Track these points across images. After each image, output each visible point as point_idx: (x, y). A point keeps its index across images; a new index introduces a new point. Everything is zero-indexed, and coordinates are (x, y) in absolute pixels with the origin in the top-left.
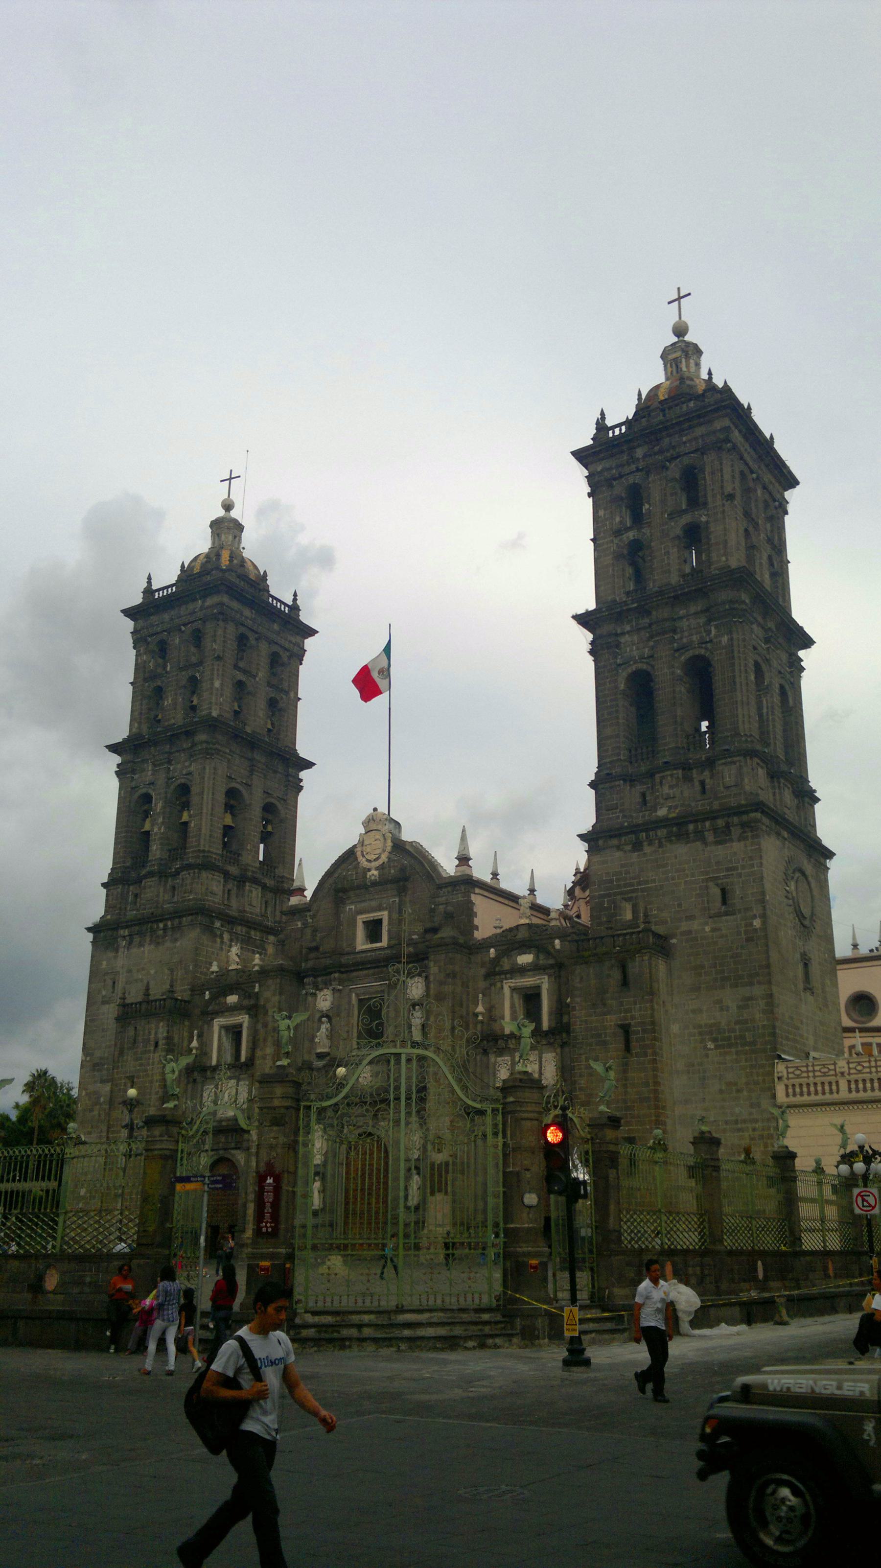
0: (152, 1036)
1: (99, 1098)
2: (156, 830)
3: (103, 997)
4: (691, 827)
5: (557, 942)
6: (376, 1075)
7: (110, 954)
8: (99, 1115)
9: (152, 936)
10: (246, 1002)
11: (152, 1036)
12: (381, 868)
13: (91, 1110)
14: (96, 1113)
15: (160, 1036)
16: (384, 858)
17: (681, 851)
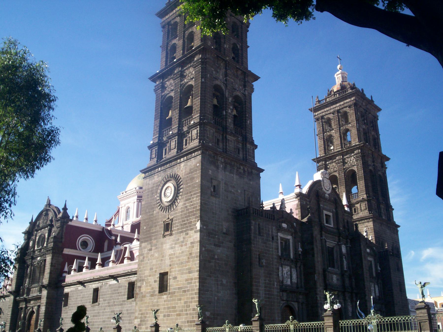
0: (270, 233)
1: (214, 255)
2: (230, 111)
3: (211, 191)
4: (389, 225)
5: (374, 248)
6: (337, 280)
7: (213, 167)
8: (215, 266)
9: (237, 170)
10: (290, 230)
11: (270, 233)
12: (329, 194)
13: (210, 262)
14: (212, 264)
15: (274, 234)
16: (329, 192)
17: (388, 231)
